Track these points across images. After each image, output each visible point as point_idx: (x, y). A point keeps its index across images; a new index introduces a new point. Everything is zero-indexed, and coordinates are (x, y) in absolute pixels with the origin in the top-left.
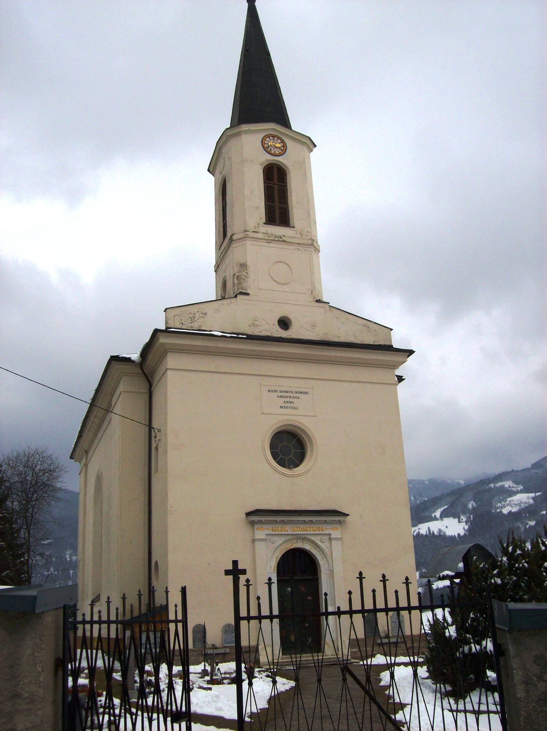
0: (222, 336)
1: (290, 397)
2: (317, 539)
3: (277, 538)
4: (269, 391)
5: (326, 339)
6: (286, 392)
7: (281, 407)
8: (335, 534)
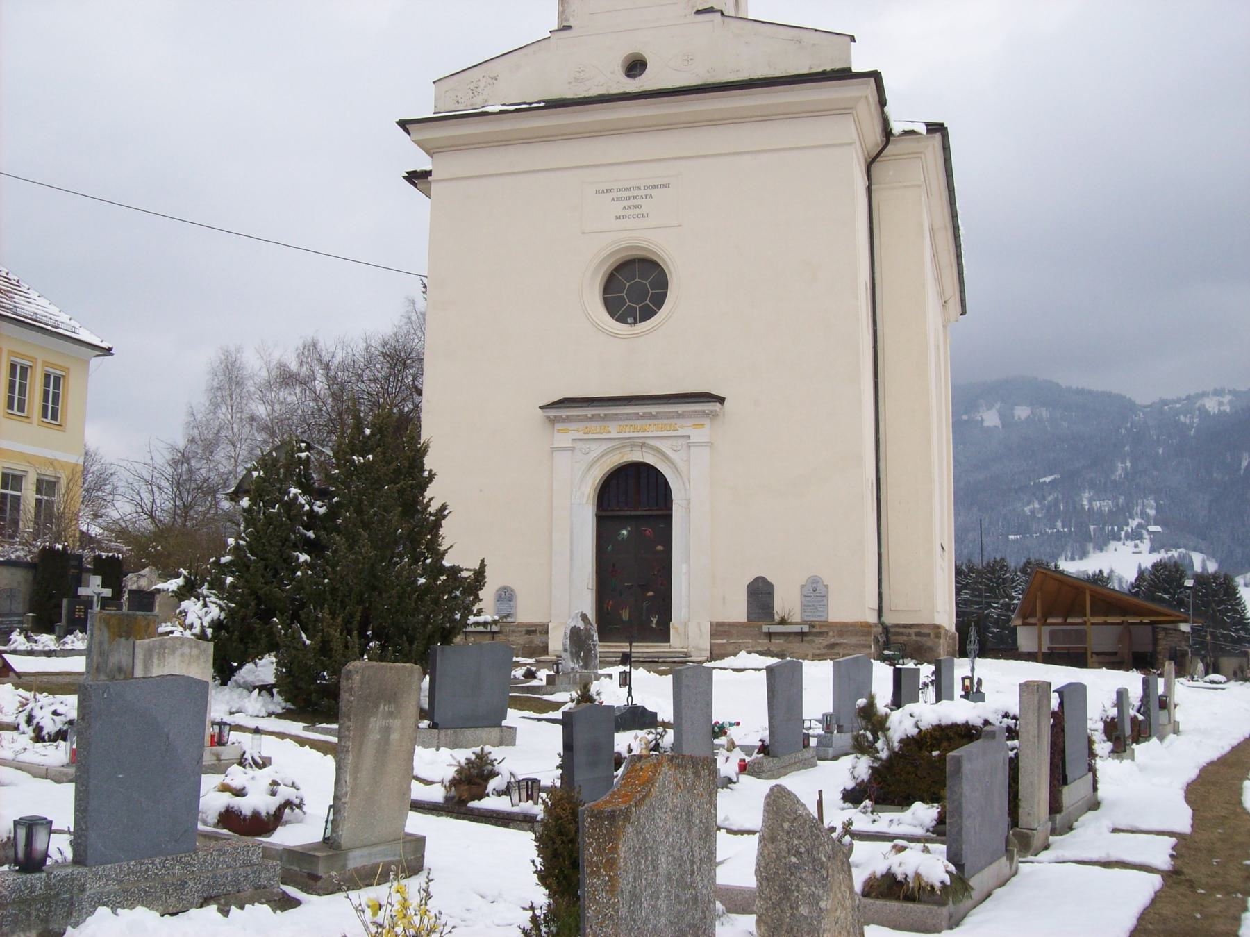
0: (502, 112)
1: (635, 197)
2: (664, 446)
3: (594, 446)
4: (598, 192)
5: (755, 77)
6: (629, 189)
7: (618, 218)
8: (698, 435)
